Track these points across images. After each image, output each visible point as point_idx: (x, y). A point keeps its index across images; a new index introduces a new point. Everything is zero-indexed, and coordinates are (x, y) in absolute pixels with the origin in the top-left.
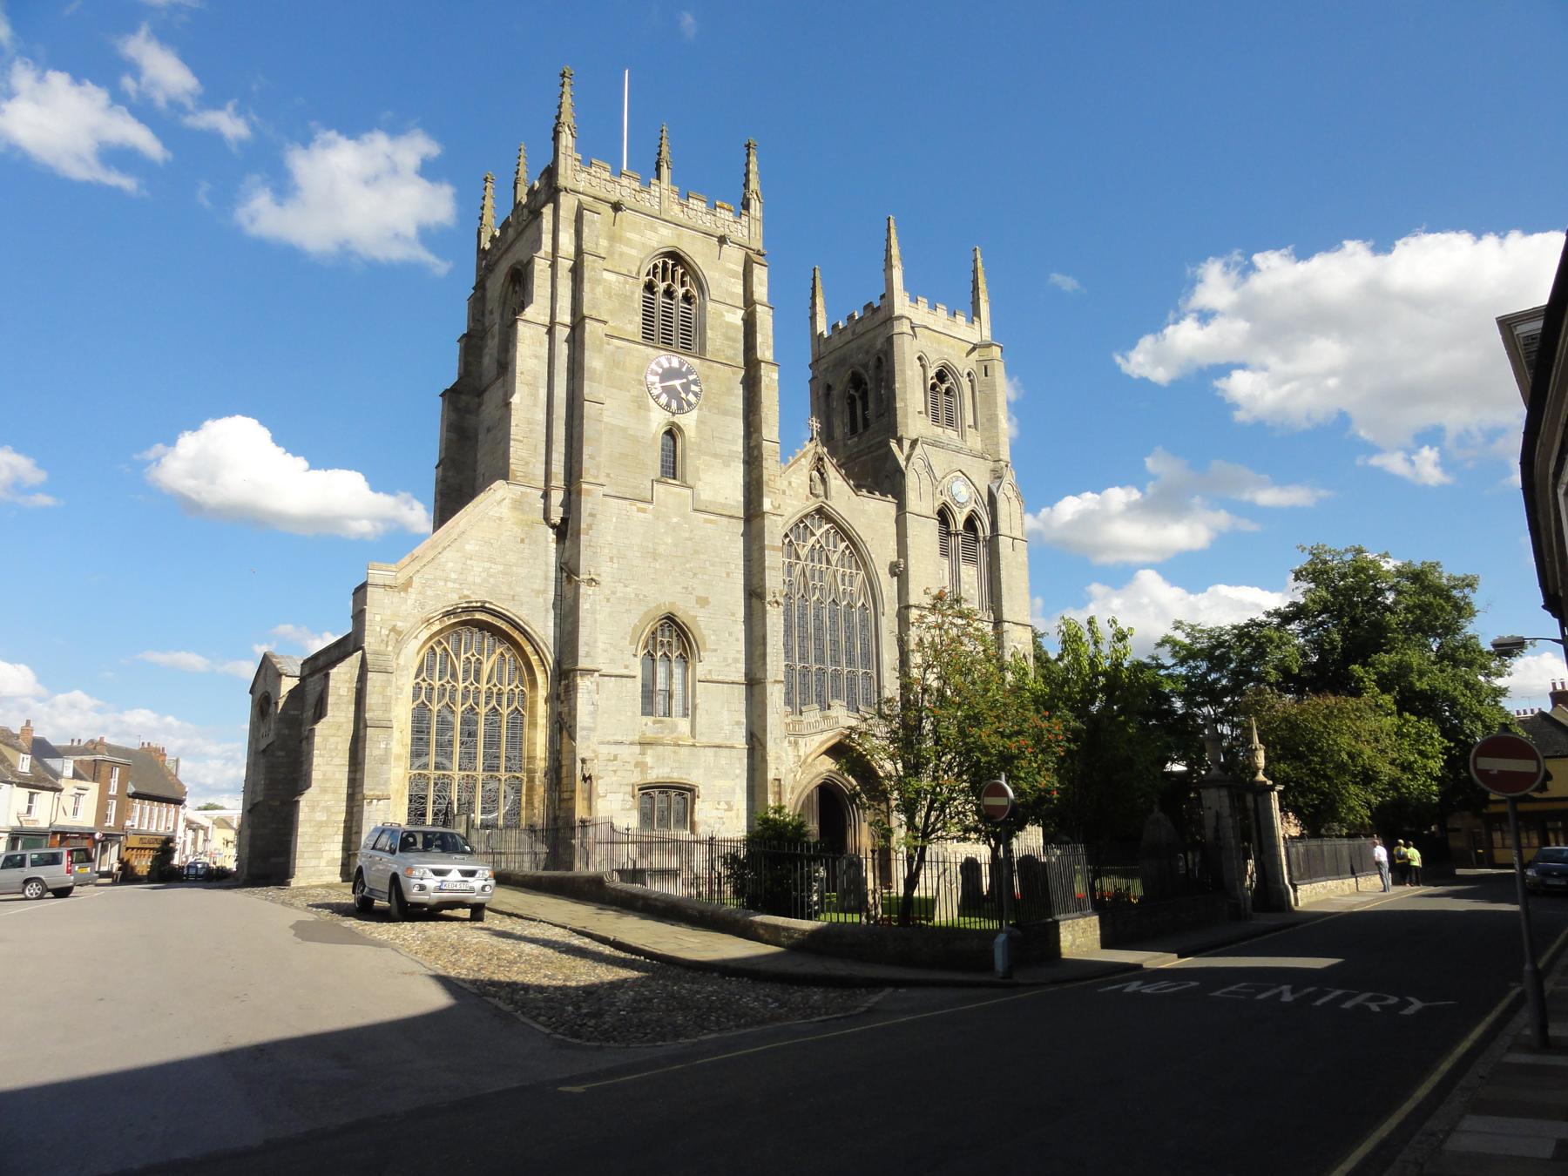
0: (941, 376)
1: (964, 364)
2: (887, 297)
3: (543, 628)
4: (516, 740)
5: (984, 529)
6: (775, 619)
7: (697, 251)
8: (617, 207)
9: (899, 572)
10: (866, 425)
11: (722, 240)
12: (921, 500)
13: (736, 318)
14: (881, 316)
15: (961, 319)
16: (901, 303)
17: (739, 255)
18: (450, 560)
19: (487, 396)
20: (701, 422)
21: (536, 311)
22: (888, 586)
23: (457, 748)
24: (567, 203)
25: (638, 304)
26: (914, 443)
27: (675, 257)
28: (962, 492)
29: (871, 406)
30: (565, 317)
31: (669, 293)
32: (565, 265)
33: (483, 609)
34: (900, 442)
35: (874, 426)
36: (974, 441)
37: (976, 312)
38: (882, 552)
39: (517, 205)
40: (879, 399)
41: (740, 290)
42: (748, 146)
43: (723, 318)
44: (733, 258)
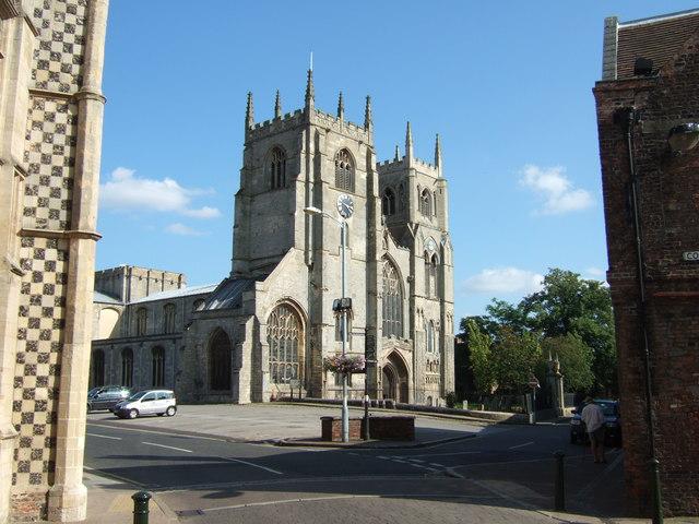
0: (424, 193)
1: (433, 188)
2: (406, 158)
3: (305, 306)
4: (295, 350)
5: (438, 262)
6: (380, 303)
7: (352, 147)
8: (328, 131)
9: (411, 281)
10: (393, 212)
11: (361, 142)
12: (419, 251)
13: (364, 176)
14: (401, 166)
15: (432, 168)
16: (413, 164)
17: (365, 149)
18: (279, 280)
19: (258, 198)
20: (354, 221)
21: (302, 176)
22: (407, 286)
23: (279, 353)
24: (312, 129)
25: (334, 173)
26: (417, 225)
27: (345, 151)
28: (431, 248)
29: (397, 205)
30: (312, 180)
31: (341, 166)
32: (312, 157)
33: (288, 299)
34: (411, 224)
35: (398, 214)
36: (435, 222)
37: (437, 164)
38: (405, 272)
39: (277, 119)
40: (401, 203)
41: (365, 164)
42: (368, 98)
43: (361, 176)
44: (363, 150)
